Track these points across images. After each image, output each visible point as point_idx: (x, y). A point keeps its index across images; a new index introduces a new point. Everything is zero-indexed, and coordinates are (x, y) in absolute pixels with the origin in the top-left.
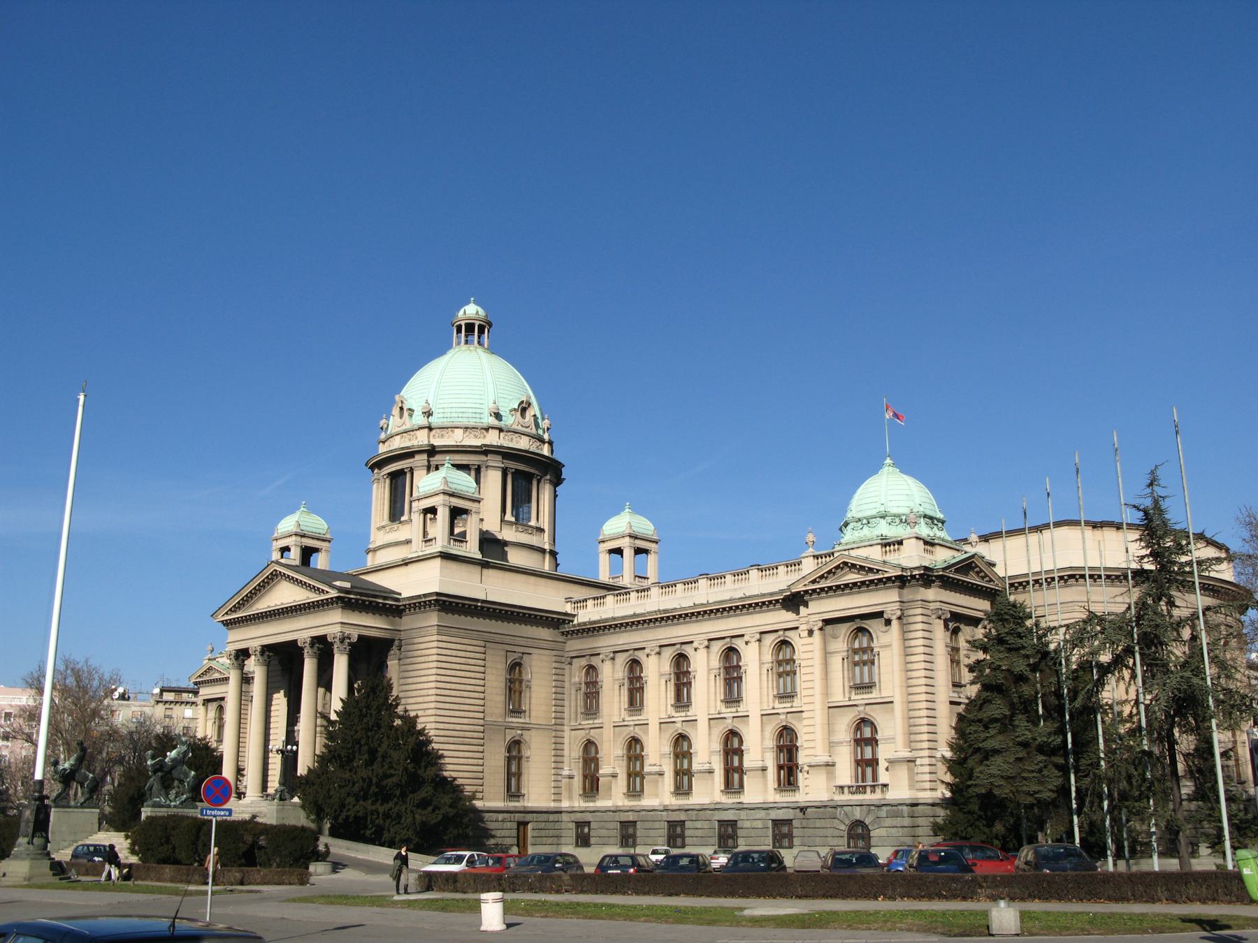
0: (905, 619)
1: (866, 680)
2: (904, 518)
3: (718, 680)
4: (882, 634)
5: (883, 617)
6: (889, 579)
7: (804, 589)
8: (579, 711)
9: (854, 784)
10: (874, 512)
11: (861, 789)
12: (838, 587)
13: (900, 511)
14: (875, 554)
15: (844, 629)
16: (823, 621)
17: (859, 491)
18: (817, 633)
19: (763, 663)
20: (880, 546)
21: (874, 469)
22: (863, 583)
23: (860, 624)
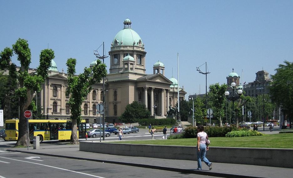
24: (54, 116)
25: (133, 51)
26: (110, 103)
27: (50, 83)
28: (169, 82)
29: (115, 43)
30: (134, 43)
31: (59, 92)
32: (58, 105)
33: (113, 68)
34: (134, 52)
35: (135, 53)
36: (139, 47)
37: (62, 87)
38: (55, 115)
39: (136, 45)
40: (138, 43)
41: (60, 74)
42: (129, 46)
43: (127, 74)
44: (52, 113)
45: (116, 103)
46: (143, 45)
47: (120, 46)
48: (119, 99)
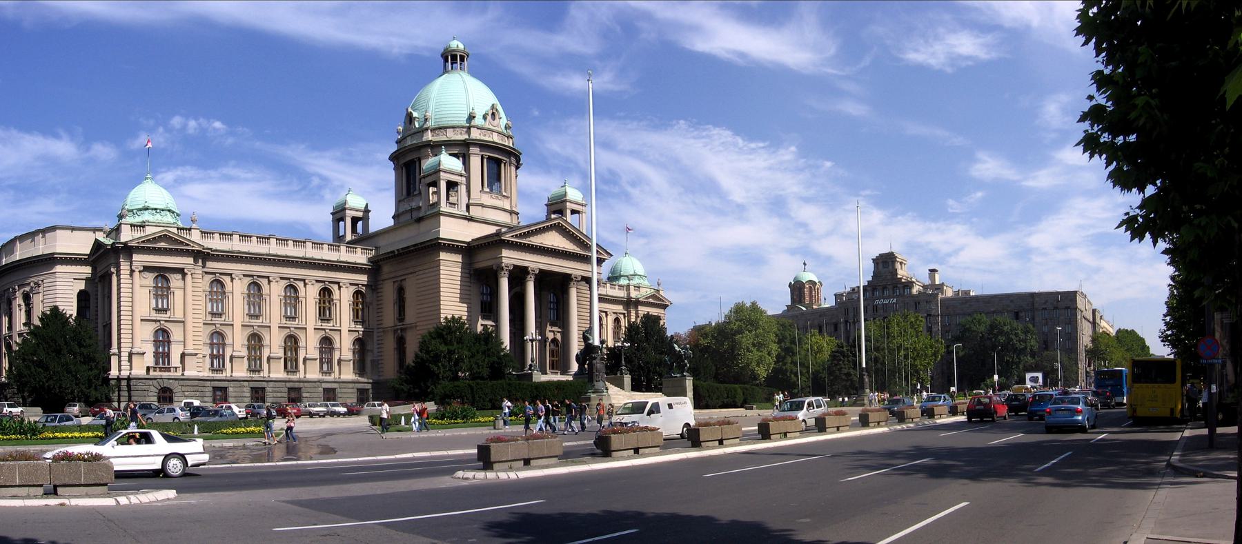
16: (143, 266)
23: (162, 274)
24: (155, 379)
25: (467, 144)
26: (385, 331)
27: (137, 266)
29: (408, 124)
30: (471, 117)
31: (178, 294)
33: (401, 210)
35: (473, 150)
36: (489, 130)
37: (188, 277)
38: (157, 374)
39: (479, 121)
40: (485, 117)
41: (185, 234)
42: (453, 127)
43: (432, 221)
44: (148, 369)
45: (402, 330)
47: (423, 130)
48: (410, 316)
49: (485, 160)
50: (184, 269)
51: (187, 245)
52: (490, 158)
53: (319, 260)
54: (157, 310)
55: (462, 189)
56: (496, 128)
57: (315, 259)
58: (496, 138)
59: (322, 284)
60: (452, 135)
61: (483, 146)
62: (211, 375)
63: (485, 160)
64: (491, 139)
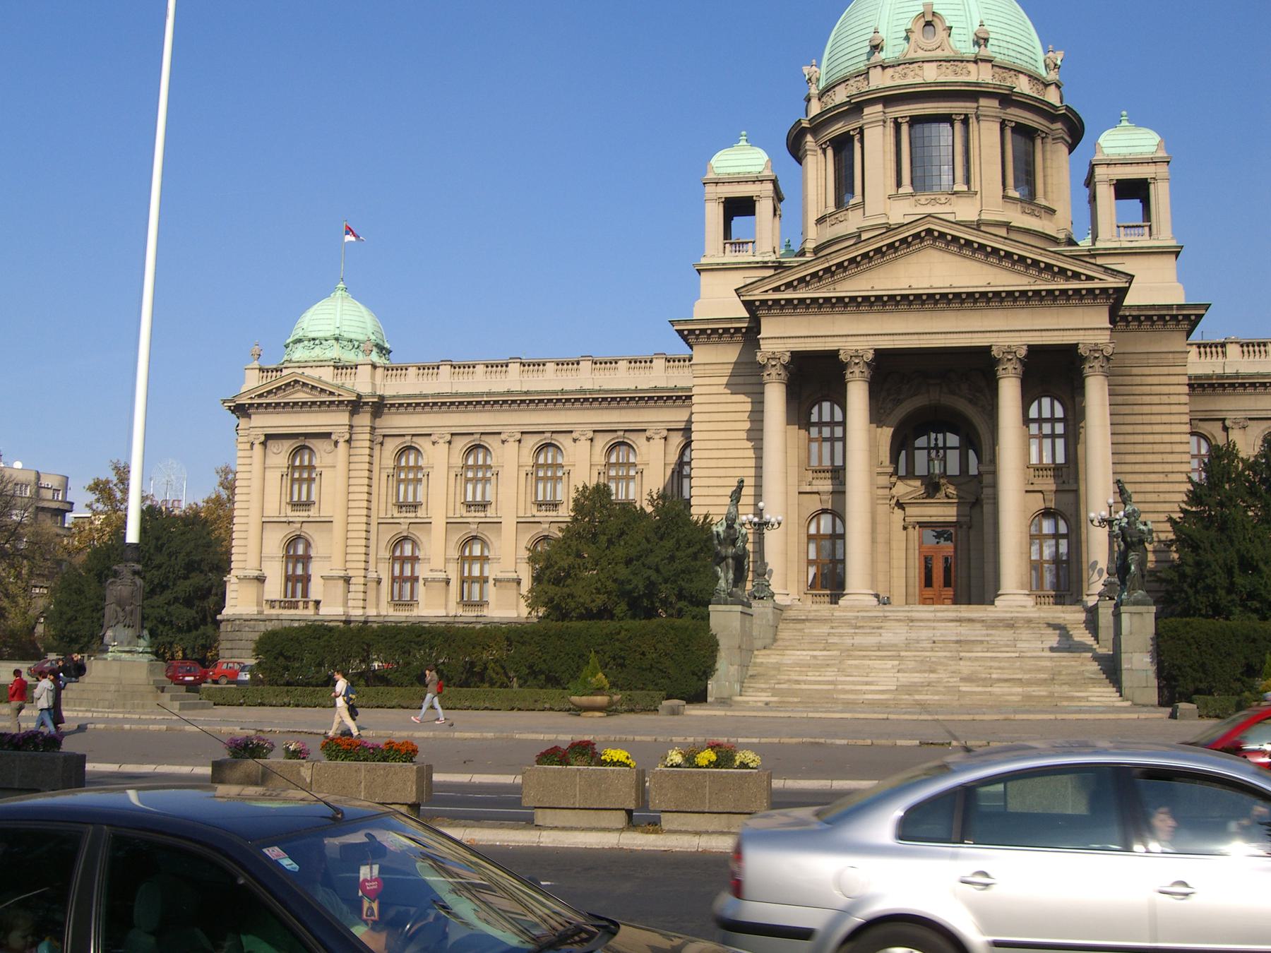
0: (352, 443)
1: (304, 498)
2: (356, 344)
3: (459, 481)
4: (324, 455)
5: (330, 438)
6: (341, 402)
7: (249, 402)
8: (390, 500)
9: (282, 599)
10: (328, 334)
11: (294, 605)
12: (287, 404)
13: (353, 336)
14: (327, 375)
15: (288, 446)
16: (266, 435)
17: (312, 310)
18: (258, 447)
19: (522, 466)
20: (332, 368)
21: (325, 293)
22: (314, 403)
23: (302, 443)
25: (855, 108)
28: (1076, 276)
30: (876, 48)
32: (313, 553)
34: (867, 111)
46: (981, 41)
49: (905, 129)
50: (331, 433)
51: (332, 393)
52: (915, 121)
53: (433, 396)
54: (296, 505)
55: (764, 208)
56: (939, 54)
57: (426, 396)
58: (930, 74)
59: (400, 440)
60: (840, 96)
61: (889, 100)
62: (391, 612)
63: (905, 129)
64: (918, 80)
